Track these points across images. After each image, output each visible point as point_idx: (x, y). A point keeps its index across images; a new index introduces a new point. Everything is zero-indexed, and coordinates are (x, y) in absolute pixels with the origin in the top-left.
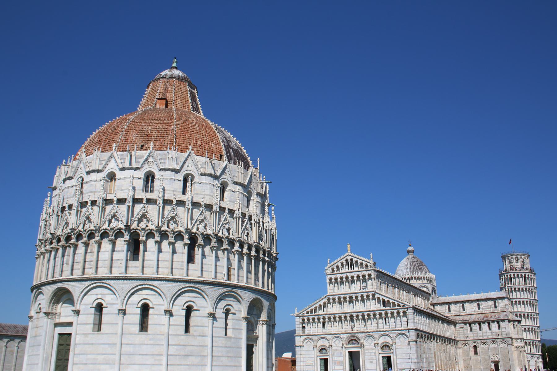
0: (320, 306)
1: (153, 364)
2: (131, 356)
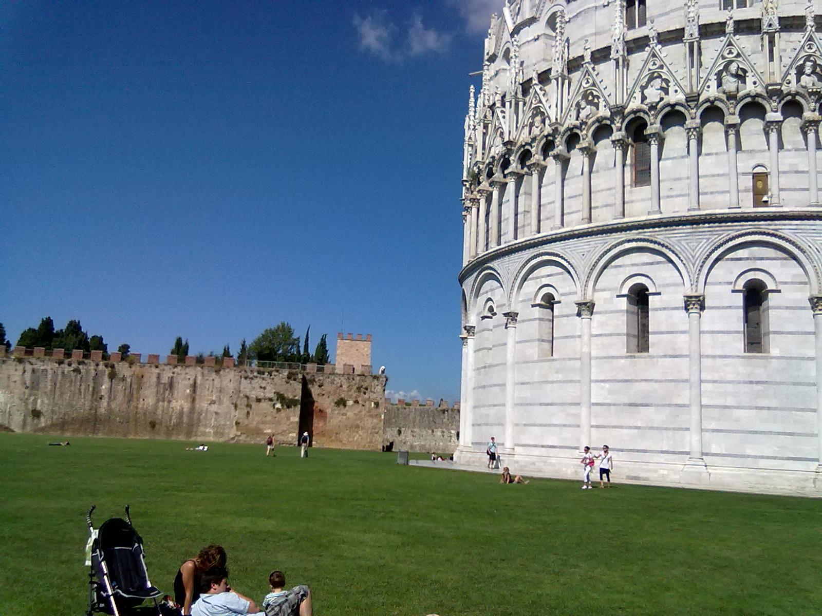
1: (565, 425)
2: (528, 408)
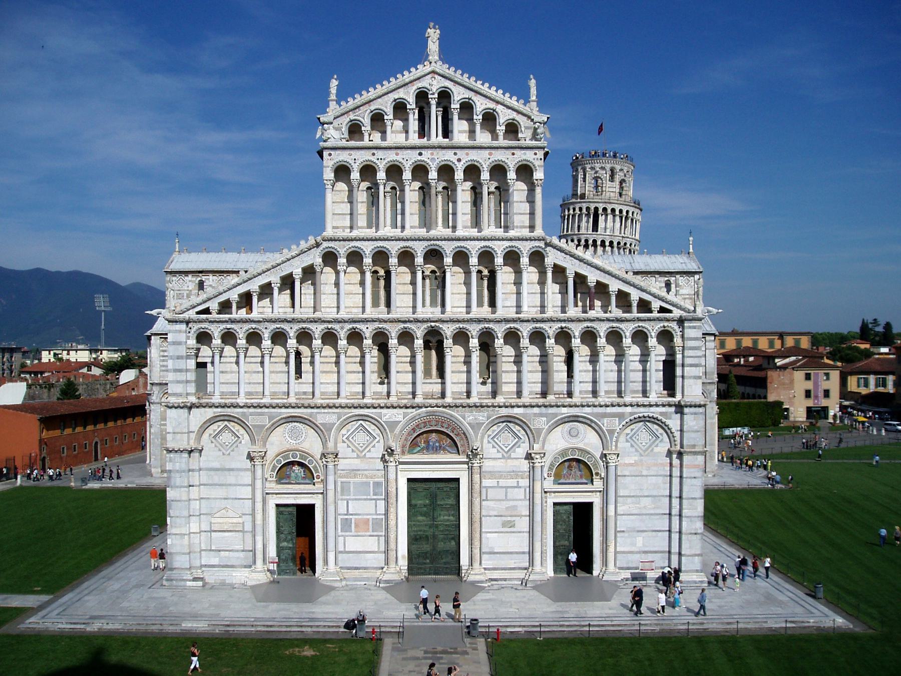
0: (288, 282)
